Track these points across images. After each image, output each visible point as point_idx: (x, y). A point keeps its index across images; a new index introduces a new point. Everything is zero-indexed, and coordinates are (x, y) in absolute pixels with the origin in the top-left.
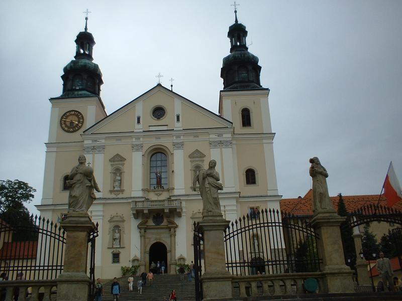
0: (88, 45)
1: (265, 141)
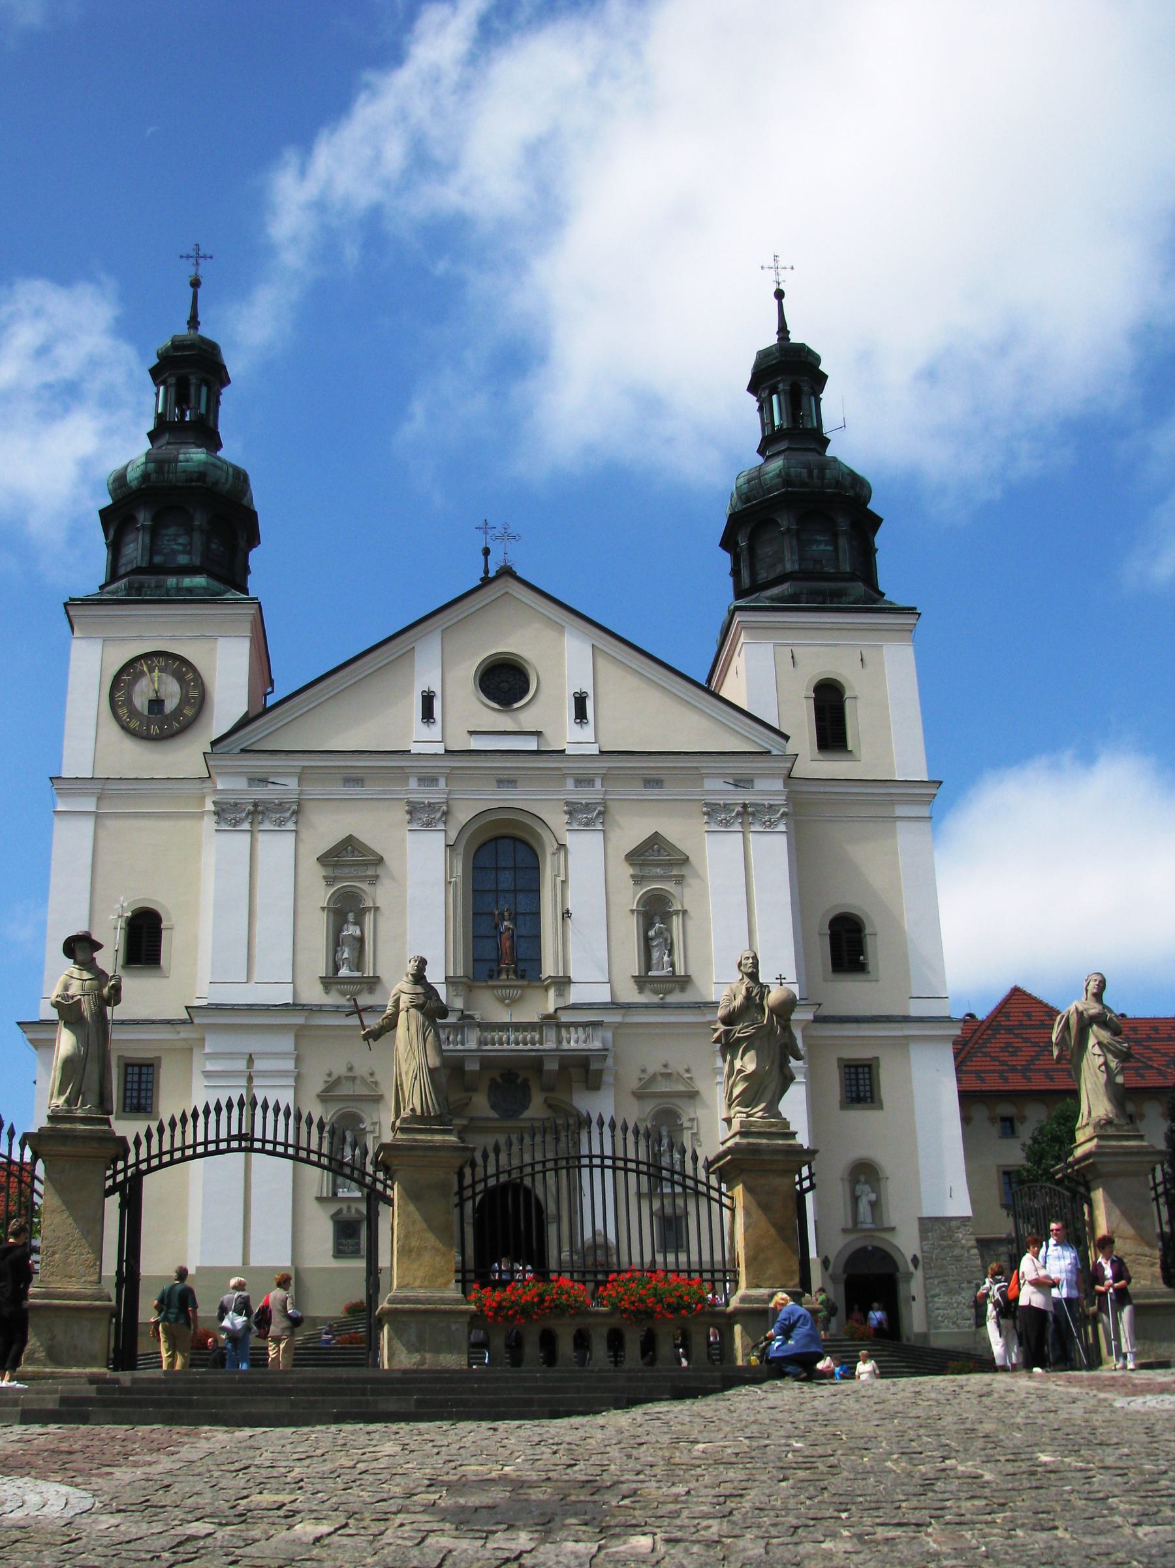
0: (204, 390)
1: (900, 811)
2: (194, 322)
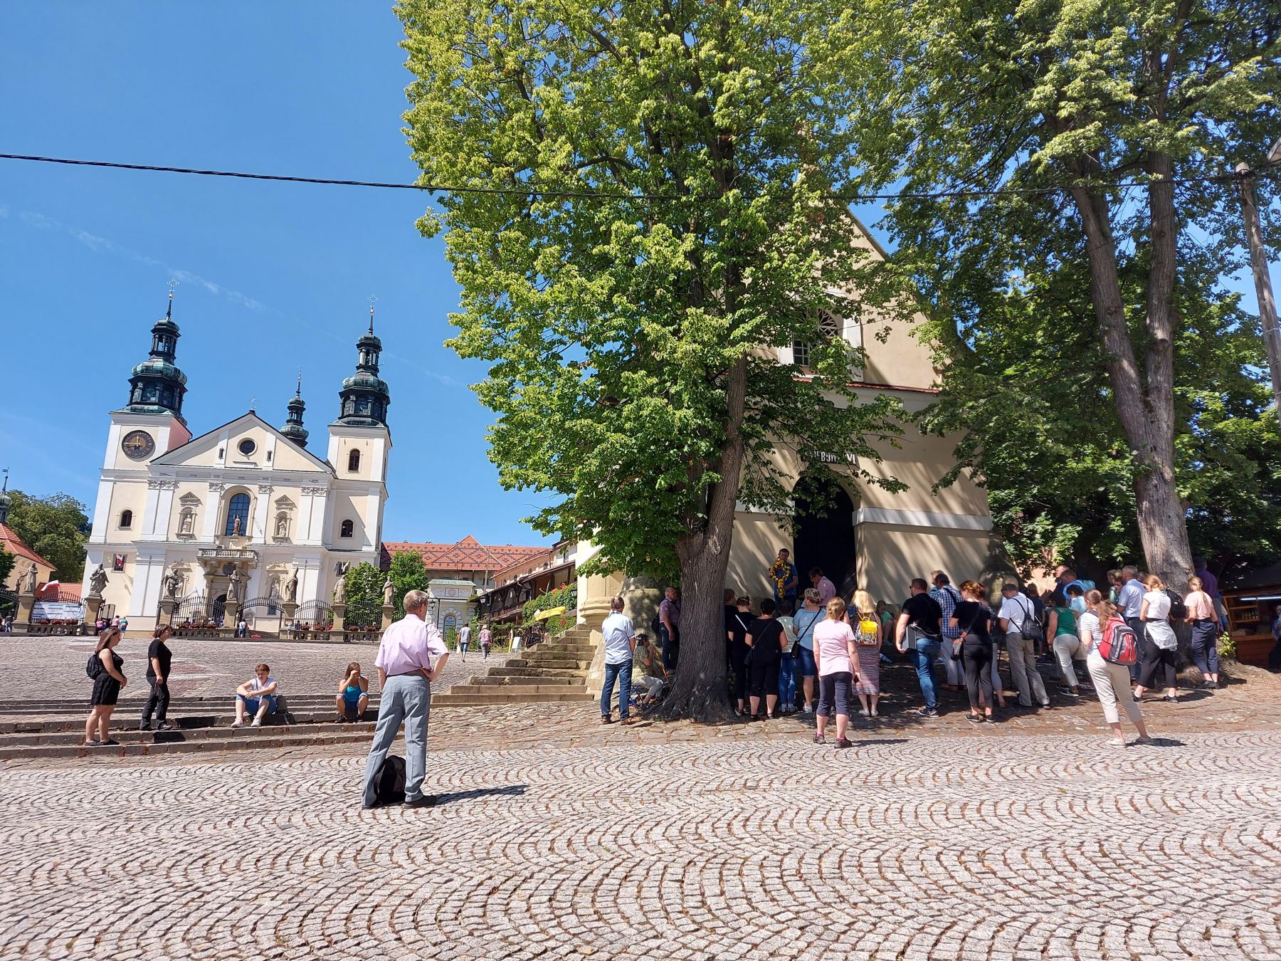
2: (169, 314)
